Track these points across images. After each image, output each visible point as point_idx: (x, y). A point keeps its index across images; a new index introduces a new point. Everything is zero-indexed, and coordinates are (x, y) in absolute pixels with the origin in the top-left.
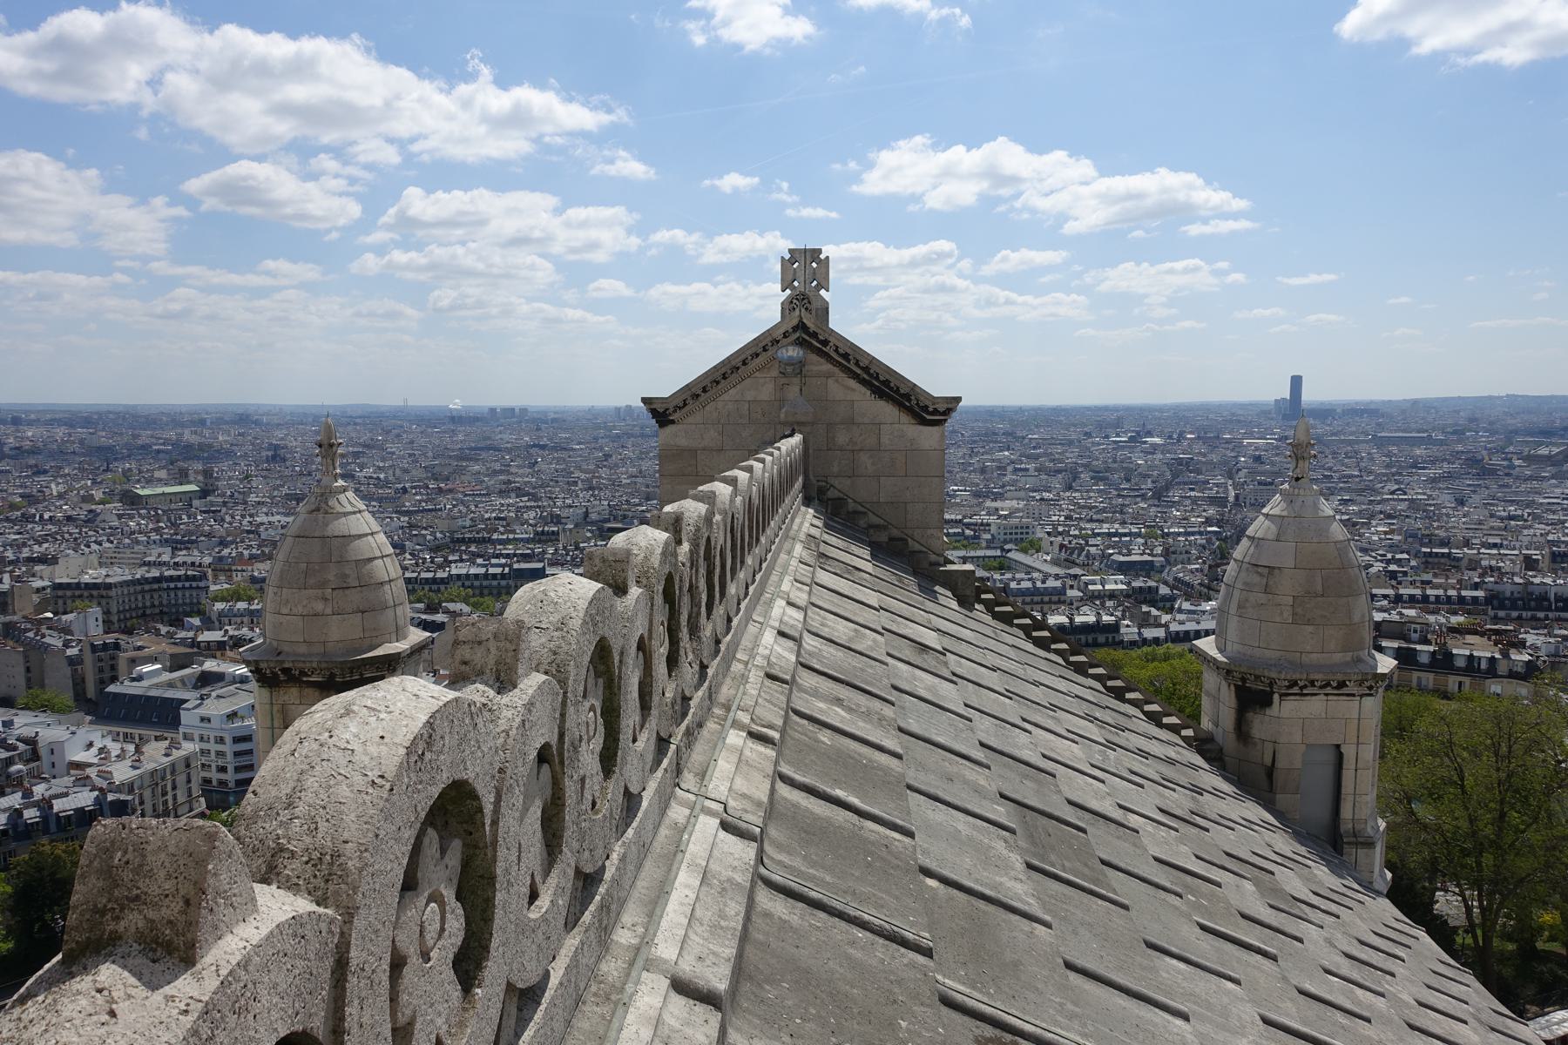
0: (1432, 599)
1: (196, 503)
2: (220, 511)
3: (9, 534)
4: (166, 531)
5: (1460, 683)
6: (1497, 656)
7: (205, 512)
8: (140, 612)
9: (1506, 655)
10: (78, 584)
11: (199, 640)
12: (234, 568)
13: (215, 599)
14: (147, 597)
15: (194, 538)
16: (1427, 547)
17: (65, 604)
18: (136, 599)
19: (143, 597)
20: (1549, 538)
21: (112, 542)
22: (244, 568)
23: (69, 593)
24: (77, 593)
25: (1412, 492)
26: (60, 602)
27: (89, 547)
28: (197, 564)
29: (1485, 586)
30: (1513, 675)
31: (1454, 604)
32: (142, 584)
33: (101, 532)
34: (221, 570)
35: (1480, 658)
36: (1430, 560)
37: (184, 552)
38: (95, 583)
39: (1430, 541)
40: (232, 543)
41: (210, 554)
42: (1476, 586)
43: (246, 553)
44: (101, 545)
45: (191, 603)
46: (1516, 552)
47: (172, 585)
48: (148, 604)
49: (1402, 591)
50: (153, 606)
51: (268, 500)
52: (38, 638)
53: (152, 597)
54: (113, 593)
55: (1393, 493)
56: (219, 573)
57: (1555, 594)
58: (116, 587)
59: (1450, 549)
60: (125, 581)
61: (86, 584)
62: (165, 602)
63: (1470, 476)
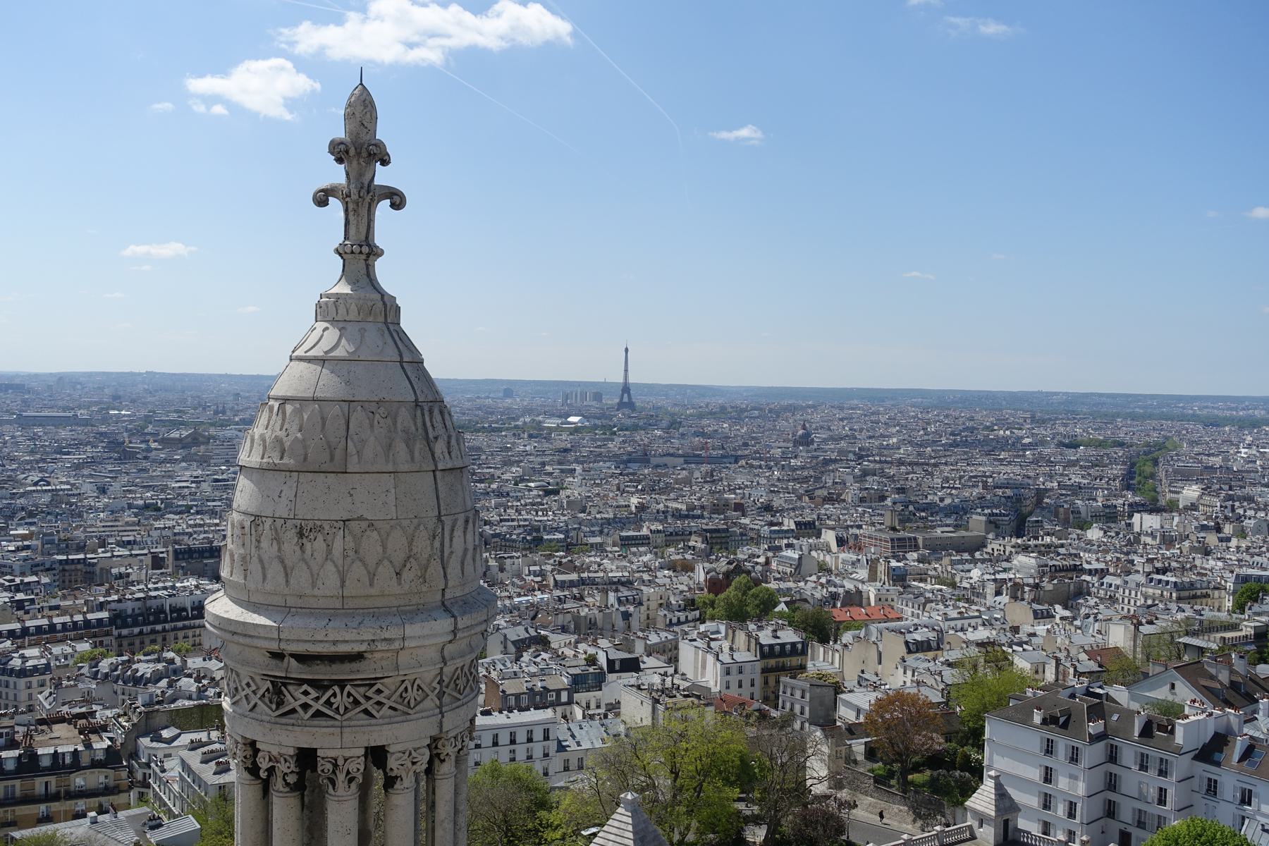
0: (59, 627)
5: (46, 783)
6: (80, 748)
9: (88, 746)
16: (63, 554)
20: (175, 531)
25: (56, 481)
29: (108, 607)
30: (95, 764)
31: (81, 629)
35: (63, 754)
36: (67, 567)
39: (67, 546)
42: (101, 607)
46: (145, 551)
49: (28, 624)
55: (36, 484)
57: (170, 605)
59: (86, 554)
63: (112, 461)
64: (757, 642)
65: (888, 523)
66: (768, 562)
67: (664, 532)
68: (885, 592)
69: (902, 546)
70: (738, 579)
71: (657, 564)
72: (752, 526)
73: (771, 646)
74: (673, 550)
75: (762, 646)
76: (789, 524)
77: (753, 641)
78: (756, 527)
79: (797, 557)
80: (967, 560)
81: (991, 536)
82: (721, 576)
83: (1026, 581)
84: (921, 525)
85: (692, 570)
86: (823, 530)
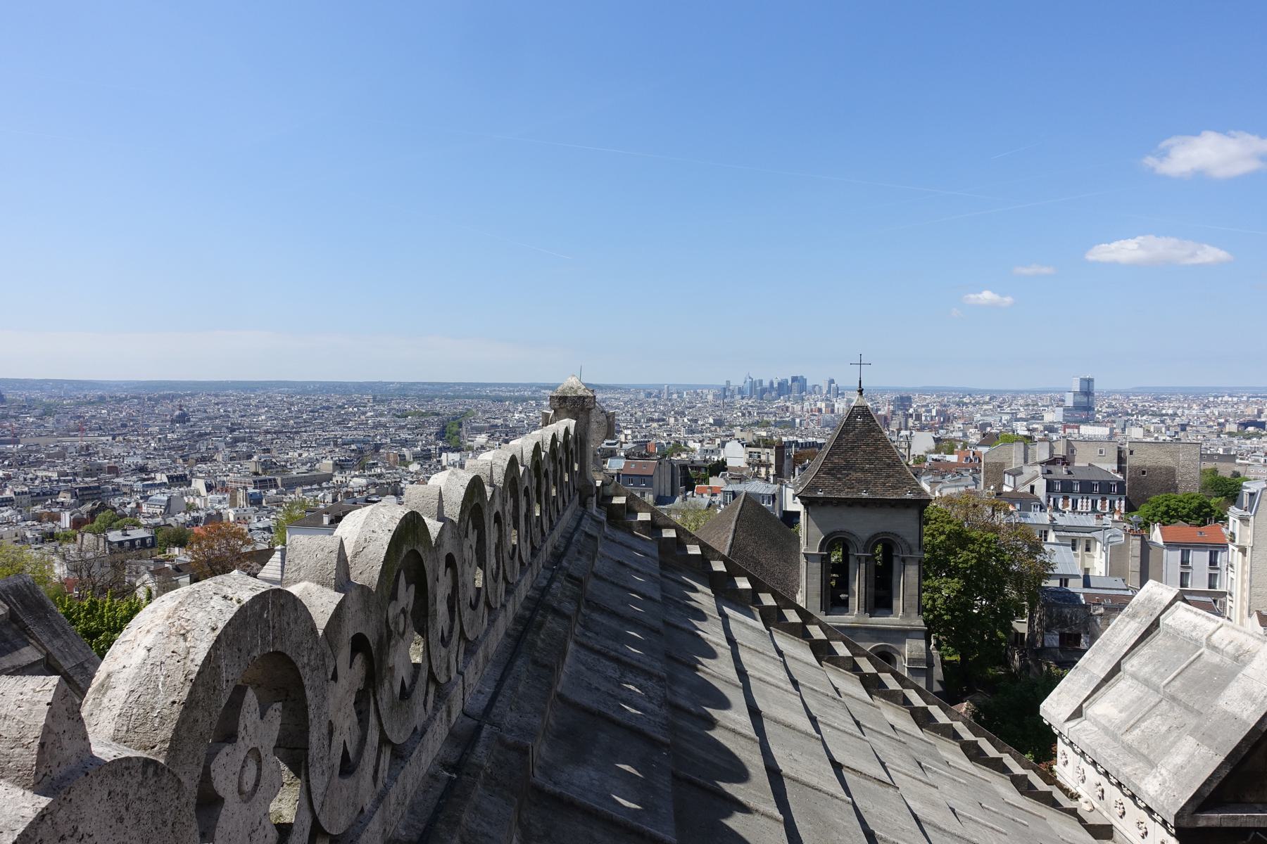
64: (106, 540)
65: (253, 469)
66: (138, 506)
67: (30, 493)
68: (242, 512)
69: (263, 484)
70: (102, 514)
71: (19, 517)
72: (125, 483)
73: (121, 543)
74: (39, 507)
75: (110, 543)
76: (161, 478)
77: (102, 540)
78: (129, 483)
79: (166, 498)
80: (315, 489)
81: (336, 473)
82: (85, 516)
83: (355, 489)
84: (280, 469)
85: (59, 519)
86: (193, 480)
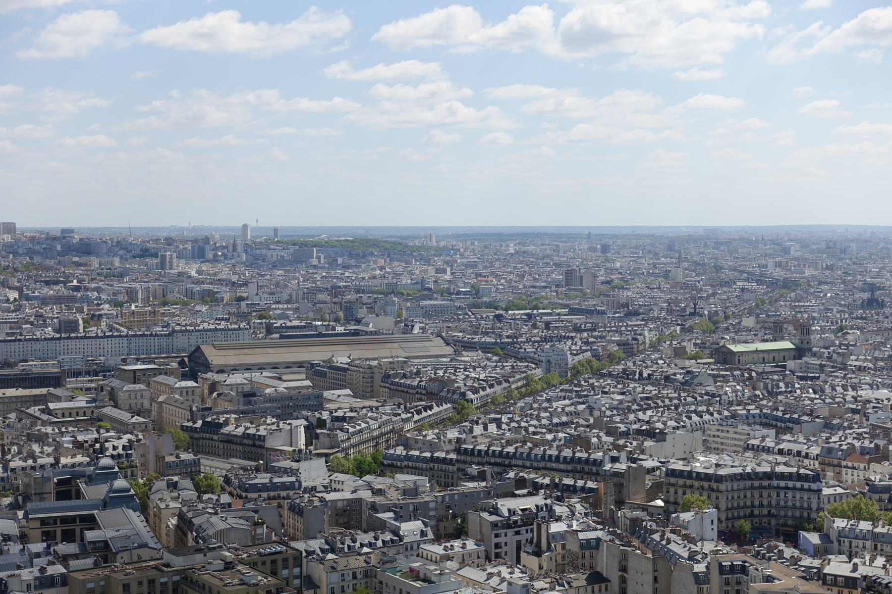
1: (791, 364)
2: (818, 378)
3: (613, 393)
4: (764, 402)
7: (802, 378)
8: (749, 511)
10: (690, 472)
11: (825, 571)
12: (844, 463)
13: (834, 514)
14: (757, 494)
15: (796, 416)
17: (676, 493)
18: (745, 497)
19: (753, 493)
21: (712, 414)
22: (856, 465)
23: (681, 482)
24: (689, 482)
26: (672, 490)
27: (690, 418)
28: (803, 454)
32: (752, 479)
33: (699, 398)
34: (830, 465)
37: (788, 437)
38: (706, 474)
40: (840, 427)
41: (816, 442)
43: (857, 444)
44: (701, 417)
45: (801, 508)
47: (782, 484)
48: (756, 503)
50: (761, 506)
51: (870, 365)
52: (664, 542)
53: (761, 496)
54: (723, 487)
56: (827, 468)
58: (726, 481)
60: (734, 474)
61: (698, 473)
62: (774, 503)
